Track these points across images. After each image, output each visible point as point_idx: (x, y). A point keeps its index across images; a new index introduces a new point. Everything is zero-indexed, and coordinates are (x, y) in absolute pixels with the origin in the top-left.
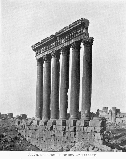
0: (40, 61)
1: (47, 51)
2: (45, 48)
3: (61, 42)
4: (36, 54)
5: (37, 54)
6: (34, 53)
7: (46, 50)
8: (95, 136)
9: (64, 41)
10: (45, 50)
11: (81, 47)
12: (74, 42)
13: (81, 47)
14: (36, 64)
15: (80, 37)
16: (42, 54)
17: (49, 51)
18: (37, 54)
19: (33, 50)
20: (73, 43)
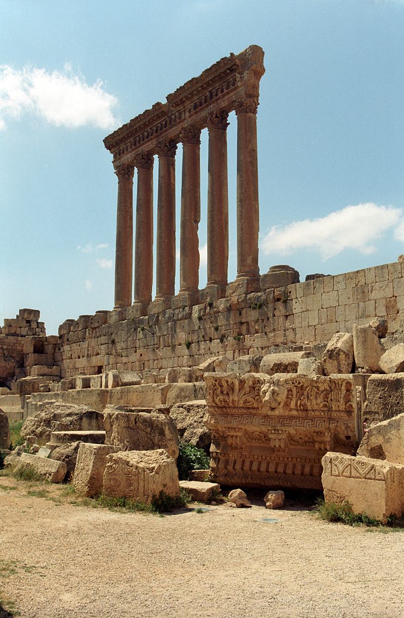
0: (124, 173)
1: (143, 144)
2: (140, 139)
4: (115, 157)
5: (118, 156)
7: (142, 142)
9: (187, 114)
10: (139, 142)
11: (229, 124)
12: (213, 112)
13: (229, 124)
14: (113, 181)
15: (226, 97)
16: (129, 155)
17: (150, 143)
18: (118, 156)
19: (108, 148)
20: (211, 114)
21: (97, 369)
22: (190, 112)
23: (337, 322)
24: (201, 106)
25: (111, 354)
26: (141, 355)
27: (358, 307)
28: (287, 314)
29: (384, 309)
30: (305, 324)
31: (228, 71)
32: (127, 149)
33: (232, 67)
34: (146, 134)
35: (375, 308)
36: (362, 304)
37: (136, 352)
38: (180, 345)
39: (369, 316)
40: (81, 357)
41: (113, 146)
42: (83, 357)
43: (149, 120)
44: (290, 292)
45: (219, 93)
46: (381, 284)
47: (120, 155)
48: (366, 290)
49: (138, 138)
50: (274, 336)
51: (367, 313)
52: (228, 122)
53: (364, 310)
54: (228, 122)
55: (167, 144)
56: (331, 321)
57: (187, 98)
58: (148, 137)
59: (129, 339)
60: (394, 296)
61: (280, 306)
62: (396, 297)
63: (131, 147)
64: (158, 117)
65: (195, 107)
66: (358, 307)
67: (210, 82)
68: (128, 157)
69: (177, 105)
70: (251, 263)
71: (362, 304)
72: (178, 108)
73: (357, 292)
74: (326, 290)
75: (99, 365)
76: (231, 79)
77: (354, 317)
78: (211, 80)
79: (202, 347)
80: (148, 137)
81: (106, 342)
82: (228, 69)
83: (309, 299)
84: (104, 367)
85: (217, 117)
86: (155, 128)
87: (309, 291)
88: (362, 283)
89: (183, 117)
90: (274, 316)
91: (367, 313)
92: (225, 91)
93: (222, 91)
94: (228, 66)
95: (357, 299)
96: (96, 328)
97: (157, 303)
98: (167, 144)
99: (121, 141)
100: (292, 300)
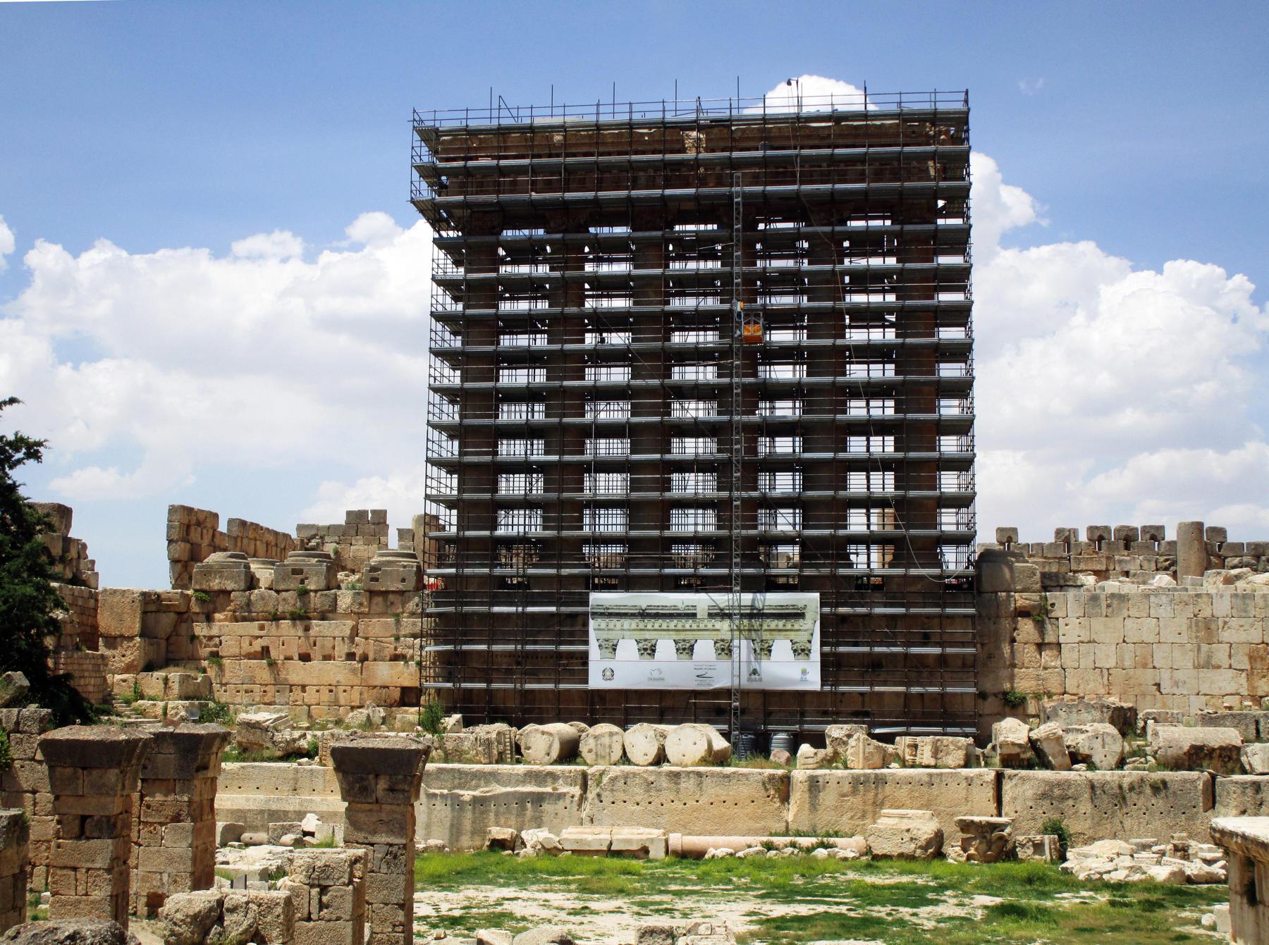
21: (396, 694)
29: (1246, 659)
30: (1086, 662)
35: (1230, 656)
36: (1205, 647)
39: (1219, 667)
44: (1053, 605)
46: (1242, 621)
48: (1213, 626)
51: (1214, 662)
53: (1209, 657)
56: (1145, 666)
66: (1199, 649)
71: (1205, 647)
73: (1197, 625)
74: (1133, 612)
75: (407, 684)
77: (1190, 665)
83: (1098, 623)
87: (1097, 610)
88: (1206, 613)
91: (1214, 662)
96: (385, 594)
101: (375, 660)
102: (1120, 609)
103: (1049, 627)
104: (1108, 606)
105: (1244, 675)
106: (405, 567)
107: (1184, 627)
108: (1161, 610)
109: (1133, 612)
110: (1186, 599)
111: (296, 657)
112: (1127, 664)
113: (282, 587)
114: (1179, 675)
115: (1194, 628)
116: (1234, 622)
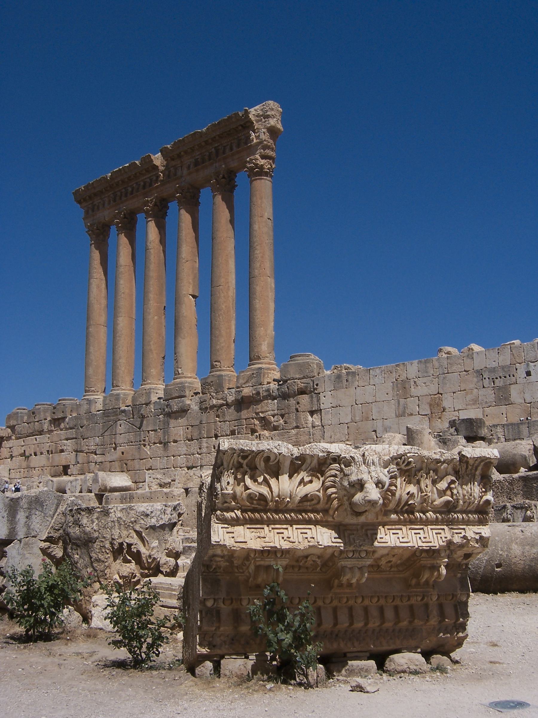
3: (175, 174)
4: (87, 212)
6: (81, 212)
7: (124, 198)
8: (298, 403)
9: (185, 172)
10: (121, 198)
11: (237, 185)
13: (237, 185)
18: (90, 211)
19: (79, 202)
22: (189, 167)
23: (373, 419)
24: (203, 163)
25: (82, 451)
26: (123, 453)
27: (399, 403)
28: (314, 409)
29: (427, 407)
31: (240, 128)
32: (104, 205)
33: (245, 124)
34: (130, 189)
36: (402, 401)
37: (115, 449)
38: (175, 441)
39: (412, 414)
40: (38, 453)
41: (85, 200)
42: (42, 453)
43: (136, 174)
44: (317, 385)
45: (227, 150)
46: (425, 380)
47: (93, 211)
48: (407, 386)
49: (119, 193)
50: (297, 434)
52: (236, 184)
54: (236, 184)
55: (158, 204)
56: (367, 419)
57: (186, 152)
58: (132, 193)
59: (106, 434)
60: (438, 393)
61: (304, 399)
62: (441, 394)
63: (109, 203)
64: (147, 171)
65: (196, 164)
66: (399, 403)
67: (217, 138)
68: (105, 215)
69: (173, 159)
70: (266, 349)
71: (402, 401)
72: (173, 163)
73: (397, 387)
76: (243, 137)
77: (394, 415)
78: (219, 135)
79: (205, 445)
80: (132, 193)
81: (74, 436)
82: (242, 126)
83: (340, 393)
84: (71, 466)
85: (224, 177)
86: (142, 184)
88: (403, 377)
89: (179, 173)
90: (297, 410)
92: (235, 149)
93: (231, 149)
94: (242, 123)
95: (397, 395)
96: (58, 419)
97: (145, 391)
98: (158, 204)
99: (95, 195)
100: (319, 393)
101: (55, 453)
102: (353, 382)
103: (315, 399)
104: (347, 381)
105: (427, 419)
106: (64, 405)
107: (390, 390)
108: (376, 379)
109: (361, 383)
110: (390, 369)
111: (33, 455)
112: (357, 418)
113: (29, 422)
114: (387, 423)
115: (396, 389)
116: (420, 382)
